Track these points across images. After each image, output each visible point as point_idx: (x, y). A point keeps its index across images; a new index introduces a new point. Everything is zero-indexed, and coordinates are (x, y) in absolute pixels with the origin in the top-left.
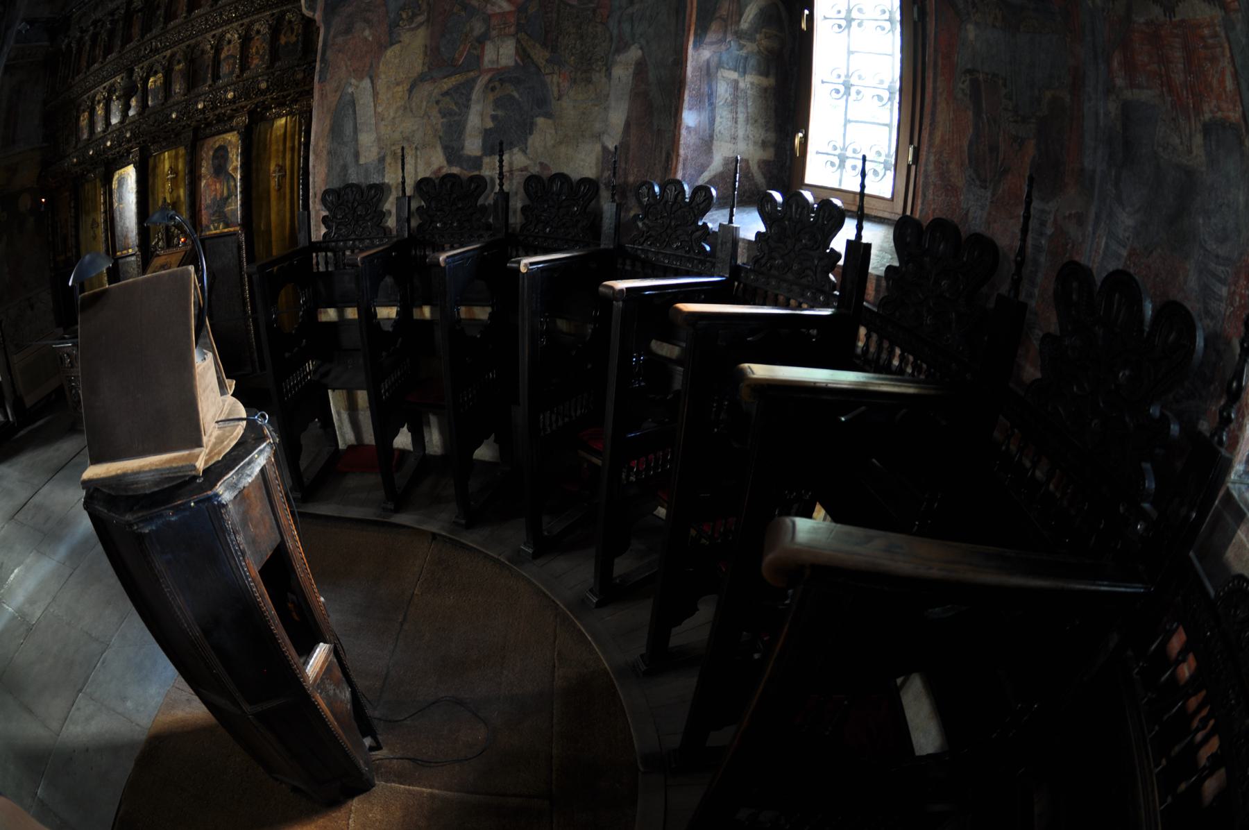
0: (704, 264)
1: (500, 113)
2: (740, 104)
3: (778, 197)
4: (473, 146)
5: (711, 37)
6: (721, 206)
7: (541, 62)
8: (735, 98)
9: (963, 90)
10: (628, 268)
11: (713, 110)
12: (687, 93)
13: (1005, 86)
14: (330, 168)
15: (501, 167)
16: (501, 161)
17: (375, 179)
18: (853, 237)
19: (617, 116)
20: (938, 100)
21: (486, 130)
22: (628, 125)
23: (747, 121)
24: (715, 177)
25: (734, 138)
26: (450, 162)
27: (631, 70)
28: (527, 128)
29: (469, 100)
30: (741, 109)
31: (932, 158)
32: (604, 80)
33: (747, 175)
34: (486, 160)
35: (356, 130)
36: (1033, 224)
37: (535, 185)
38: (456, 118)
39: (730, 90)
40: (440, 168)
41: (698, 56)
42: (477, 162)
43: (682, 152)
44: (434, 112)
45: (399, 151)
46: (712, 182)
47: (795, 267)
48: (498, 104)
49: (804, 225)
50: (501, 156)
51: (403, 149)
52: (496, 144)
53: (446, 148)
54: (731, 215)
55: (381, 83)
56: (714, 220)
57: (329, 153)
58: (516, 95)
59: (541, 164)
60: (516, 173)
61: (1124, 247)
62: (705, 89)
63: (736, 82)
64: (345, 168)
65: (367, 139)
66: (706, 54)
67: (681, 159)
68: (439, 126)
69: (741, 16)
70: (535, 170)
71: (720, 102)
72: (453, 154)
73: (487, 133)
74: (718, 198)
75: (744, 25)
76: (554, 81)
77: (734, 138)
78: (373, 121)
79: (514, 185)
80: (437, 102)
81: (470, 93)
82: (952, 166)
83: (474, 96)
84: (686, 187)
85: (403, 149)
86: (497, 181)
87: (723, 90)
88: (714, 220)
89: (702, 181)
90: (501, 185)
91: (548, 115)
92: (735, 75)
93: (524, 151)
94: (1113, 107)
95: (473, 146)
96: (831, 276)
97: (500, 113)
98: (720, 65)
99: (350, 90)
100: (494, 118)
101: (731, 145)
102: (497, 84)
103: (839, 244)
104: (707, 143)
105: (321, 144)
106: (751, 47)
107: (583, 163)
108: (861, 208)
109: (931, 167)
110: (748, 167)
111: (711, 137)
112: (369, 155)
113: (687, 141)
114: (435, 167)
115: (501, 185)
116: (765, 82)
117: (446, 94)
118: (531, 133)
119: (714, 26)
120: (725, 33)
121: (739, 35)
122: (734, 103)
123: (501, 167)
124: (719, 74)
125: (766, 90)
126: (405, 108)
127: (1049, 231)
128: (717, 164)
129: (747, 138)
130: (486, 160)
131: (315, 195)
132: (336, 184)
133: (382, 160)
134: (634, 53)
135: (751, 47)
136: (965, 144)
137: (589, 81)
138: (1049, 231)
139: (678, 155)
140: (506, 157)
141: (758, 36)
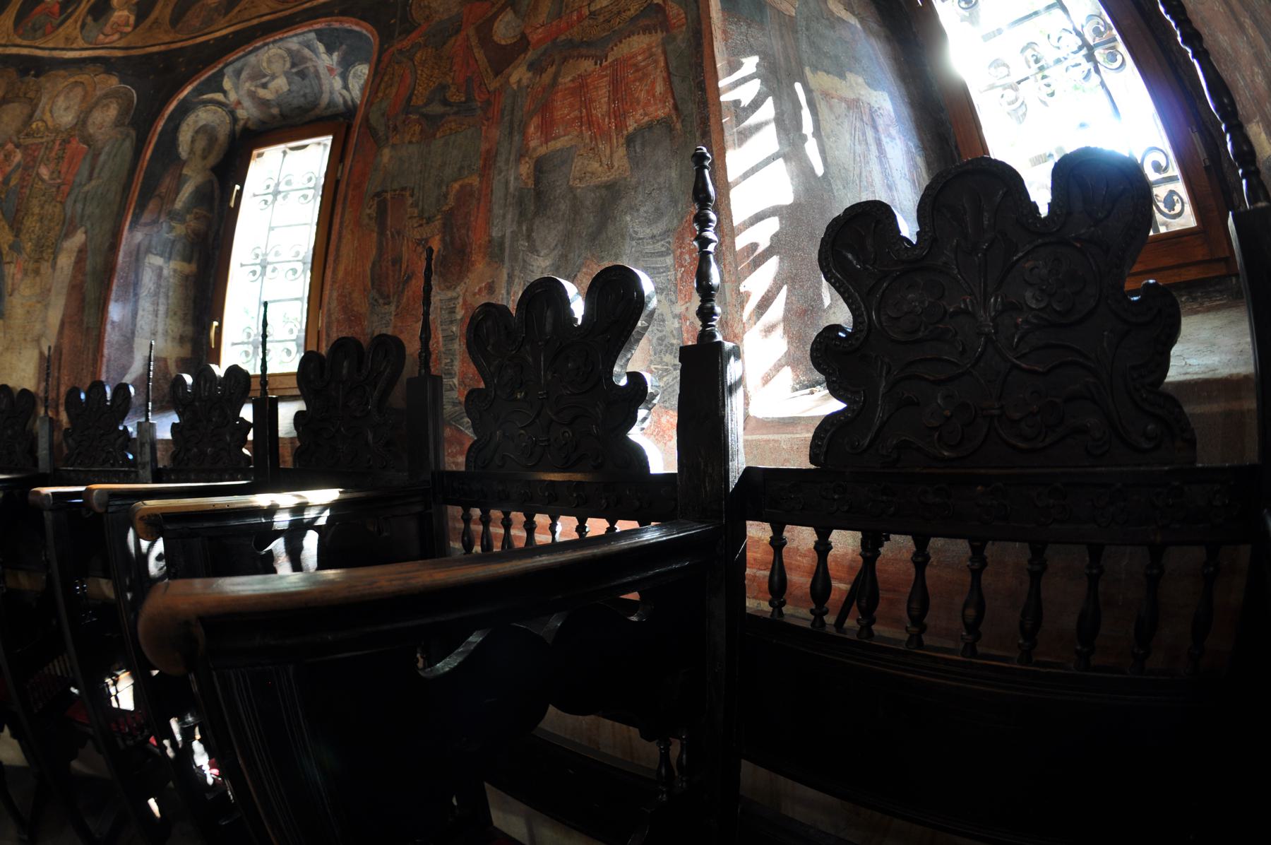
8: (159, 286)
11: (136, 302)
12: (115, 281)
25: (154, 334)
39: (155, 278)
63: (161, 269)
67: (105, 360)
71: (144, 292)
87: (148, 279)
111: (133, 333)
122: (156, 294)
135: (180, 229)
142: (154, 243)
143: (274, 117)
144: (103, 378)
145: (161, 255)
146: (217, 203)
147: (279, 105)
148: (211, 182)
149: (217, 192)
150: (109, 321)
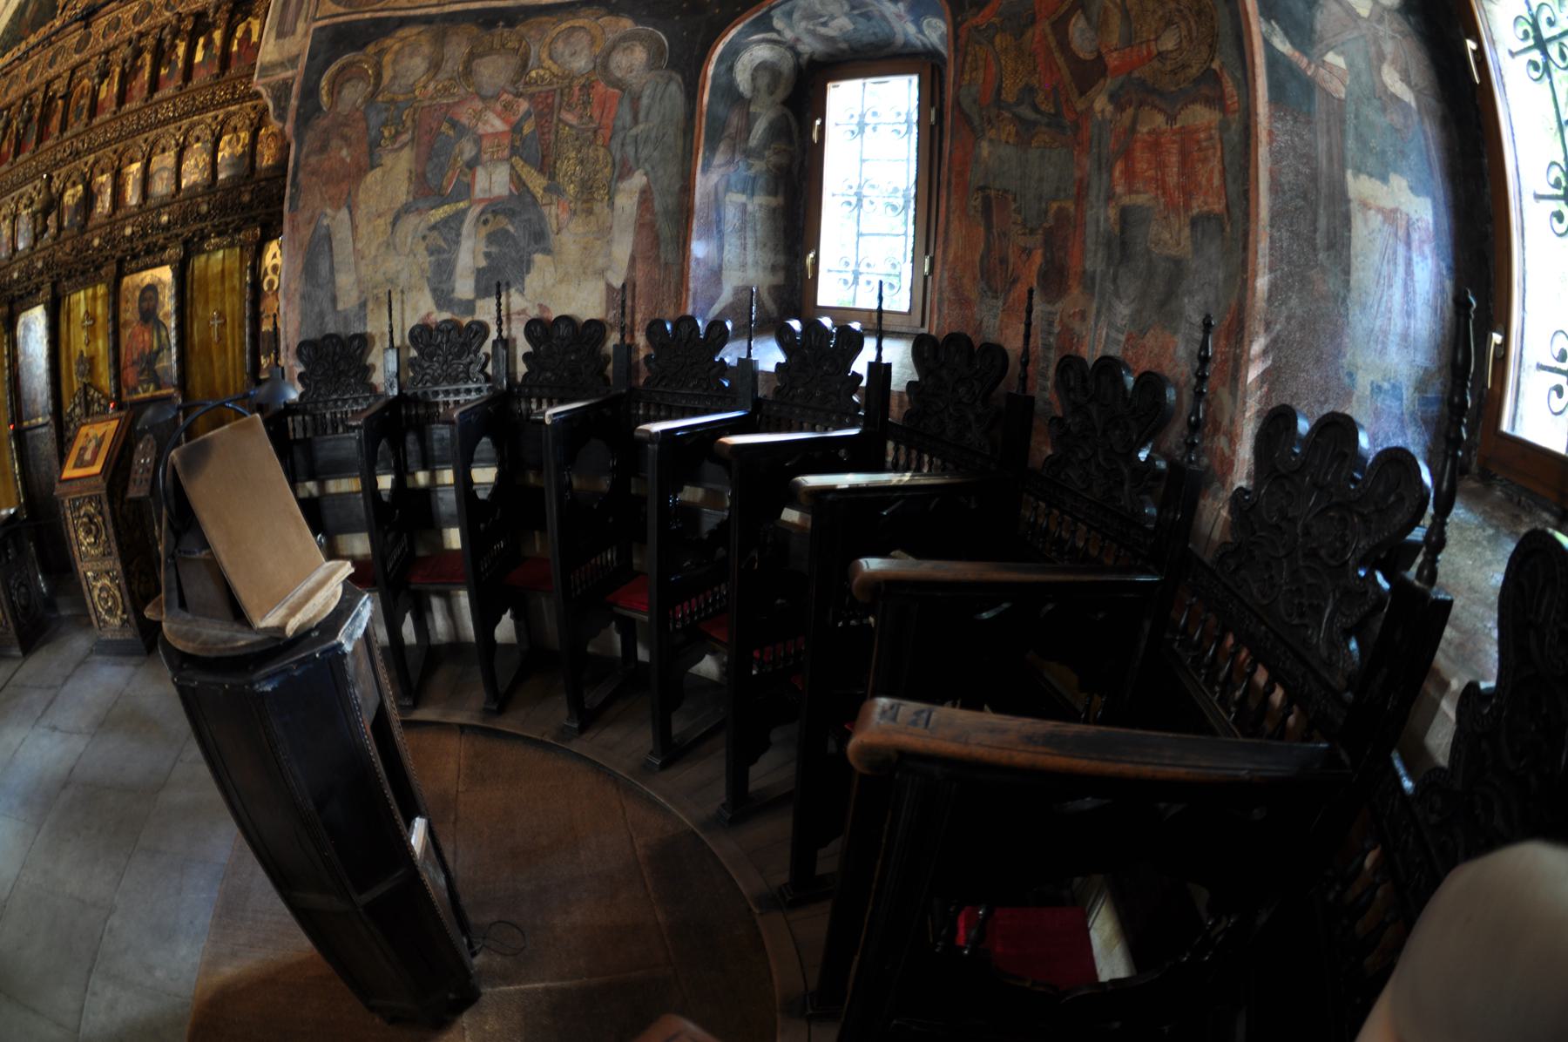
1: (494, 249)
4: (464, 288)
5: (719, 159)
7: (539, 192)
8: (744, 222)
14: (304, 315)
15: (499, 311)
16: (499, 304)
17: (356, 329)
22: (633, 259)
23: (756, 244)
25: (743, 266)
27: (636, 198)
28: (525, 266)
29: (459, 235)
32: (607, 210)
34: (480, 303)
35: (332, 270)
38: (445, 256)
39: (739, 214)
40: (428, 315)
41: (704, 184)
42: (469, 307)
43: (691, 285)
44: (421, 249)
48: (492, 238)
49: (823, 350)
50: (499, 299)
52: (494, 282)
53: (434, 291)
54: (750, 348)
56: (731, 355)
57: (303, 297)
58: (511, 228)
59: (540, 306)
63: (744, 205)
64: (321, 315)
66: (714, 177)
68: (426, 266)
69: (749, 132)
70: (534, 313)
72: (443, 298)
73: (480, 273)
75: (753, 142)
76: (553, 213)
80: (424, 238)
84: (700, 323)
87: (731, 216)
88: (731, 355)
90: (500, 330)
91: (547, 251)
92: (742, 198)
93: (521, 292)
95: (464, 288)
98: (728, 189)
100: (487, 255)
102: (490, 216)
103: (860, 366)
104: (716, 274)
105: (293, 286)
106: (759, 166)
107: (584, 302)
111: (720, 267)
112: (348, 300)
113: (696, 275)
114: (423, 313)
117: (433, 228)
118: (528, 272)
119: (722, 147)
121: (748, 154)
122: (743, 228)
123: (499, 311)
125: (774, 211)
126: (388, 245)
128: (726, 296)
129: (756, 263)
130: (480, 303)
131: (287, 348)
132: (313, 334)
133: (363, 305)
134: (638, 180)
135: (759, 166)
137: (590, 212)
140: (503, 300)
143: (843, 51)
144: (689, 312)
145: (743, 191)
146: (796, 136)
147: (846, 41)
148: (785, 115)
149: (794, 125)
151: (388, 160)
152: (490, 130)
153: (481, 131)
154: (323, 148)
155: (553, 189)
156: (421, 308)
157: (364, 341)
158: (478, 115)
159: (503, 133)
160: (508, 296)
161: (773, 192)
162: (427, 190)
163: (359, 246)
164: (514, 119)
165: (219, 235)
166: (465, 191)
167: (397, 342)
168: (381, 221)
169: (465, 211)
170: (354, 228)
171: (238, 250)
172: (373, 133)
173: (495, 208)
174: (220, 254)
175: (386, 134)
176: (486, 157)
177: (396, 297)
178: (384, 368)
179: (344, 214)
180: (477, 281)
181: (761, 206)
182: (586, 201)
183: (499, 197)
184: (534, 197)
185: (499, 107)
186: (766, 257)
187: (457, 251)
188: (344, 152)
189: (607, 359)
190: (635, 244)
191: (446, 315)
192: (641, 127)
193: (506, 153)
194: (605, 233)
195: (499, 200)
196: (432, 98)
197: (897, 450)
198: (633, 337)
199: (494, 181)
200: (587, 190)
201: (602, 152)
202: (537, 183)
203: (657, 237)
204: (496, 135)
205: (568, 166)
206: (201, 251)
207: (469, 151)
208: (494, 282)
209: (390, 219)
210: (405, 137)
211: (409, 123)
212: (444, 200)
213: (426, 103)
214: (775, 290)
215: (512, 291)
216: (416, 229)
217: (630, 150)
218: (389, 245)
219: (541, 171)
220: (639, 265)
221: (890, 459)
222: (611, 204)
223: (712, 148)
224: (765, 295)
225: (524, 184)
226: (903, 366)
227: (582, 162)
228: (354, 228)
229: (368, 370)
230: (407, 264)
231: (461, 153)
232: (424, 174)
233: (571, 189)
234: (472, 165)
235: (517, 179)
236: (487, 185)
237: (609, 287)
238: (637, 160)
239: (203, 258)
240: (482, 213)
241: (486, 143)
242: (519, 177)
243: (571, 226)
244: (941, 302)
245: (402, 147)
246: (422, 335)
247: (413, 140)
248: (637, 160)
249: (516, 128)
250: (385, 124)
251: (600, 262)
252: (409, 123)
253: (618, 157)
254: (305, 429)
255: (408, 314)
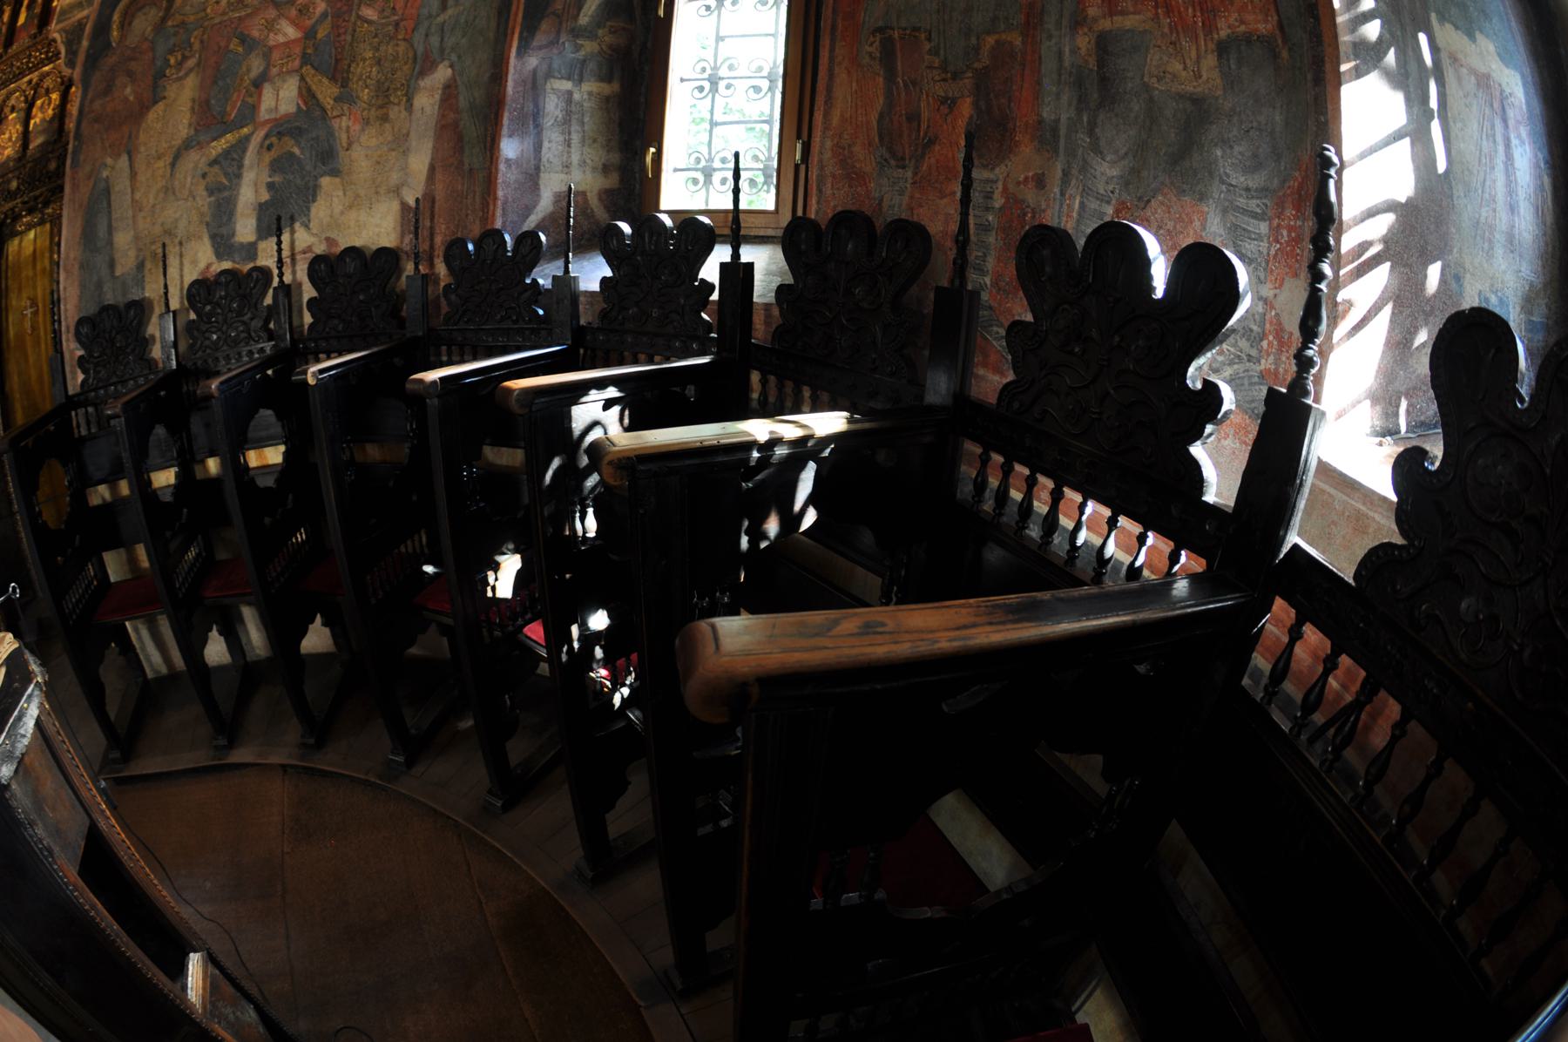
0: (537, 333)
1: (277, 179)
2: (574, 122)
3: (626, 228)
4: (245, 229)
5: (540, 39)
6: (554, 257)
7: (328, 102)
8: (568, 113)
9: (870, 54)
10: (445, 358)
12: (506, 115)
13: (929, 39)
14: (83, 286)
15: (280, 251)
16: (279, 243)
17: (135, 295)
18: (728, 259)
19: (419, 161)
20: (837, 70)
21: (261, 205)
22: (432, 169)
23: (583, 141)
24: (544, 219)
26: (220, 256)
27: (437, 97)
28: (310, 193)
29: (241, 167)
30: (575, 127)
31: (829, 144)
32: (404, 114)
33: (584, 210)
34: (262, 245)
35: (110, 230)
36: (976, 196)
37: (324, 268)
38: (226, 194)
40: (208, 267)
41: (520, 66)
42: (251, 250)
43: (500, 193)
44: (201, 191)
45: (160, 251)
46: (542, 226)
47: (655, 313)
48: (275, 167)
49: (661, 257)
50: (279, 237)
51: (164, 245)
53: (213, 237)
54: (567, 263)
55: (140, 159)
58: (296, 151)
59: (328, 239)
60: (298, 257)
61: (1108, 202)
62: (530, 107)
63: (570, 93)
64: (99, 285)
65: (122, 239)
66: (533, 61)
68: (205, 209)
69: (580, 9)
70: (320, 249)
71: (548, 122)
72: (223, 244)
73: (262, 208)
74: (550, 247)
76: (343, 125)
77: (567, 167)
78: (130, 213)
79: (300, 273)
80: (204, 176)
81: (242, 158)
82: (857, 149)
83: (247, 162)
84: (507, 238)
85: (164, 245)
86: (276, 272)
87: (552, 106)
88: (544, 276)
89: (530, 223)
90: (281, 275)
91: (335, 173)
92: (567, 85)
93: (307, 227)
94: (1084, 42)
95: (245, 229)
96: (704, 316)
97: (277, 179)
98: (549, 75)
99: (105, 174)
100: (271, 186)
101: (563, 176)
102: (274, 140)
103: (710, 271)
106: (590, 47)
107: (377, 228)
108: (735, 227)
109: (828, 155)
110: (586, 201)
112: (126, 263)
113: (507, 177)
114: (202, 265)
115: (281, 275)
116: (606, 89)
119: (544, 26)
120: (558, 33)
121: (576, 33)
122: (566, 122)
123: (280, 251)
124: (548, 86)
125: (607, 99)
126: (167, 189)
127: (998, 202)
128: (546, 203)
130: (262, 245)
133: (140, 266)
134: (443, 73)
135: (590, 47)
136: (874, 118)
137: (385, 119)
138: (998, 202)
139: (496, 199)
140: (285, 237)
141: (600, 32)
142: (555, 66)
145: (569, 79)
150: (502, 159)
151: (171, 91)
152: (281, 39)
153: (272, 43)
154: (108, 90)
155: (346, 98)
156: (201, 260)
157: (140, 308)
158: (270, 26)
159: (294, 41)
160: (293, 232)
161: (607, 78)
162: (210, 119)
163: (138, 196)
164: (309, 23)
165: (30, 212)
166: (249, 113)
167: (175, 304)
168: (161, 164)
169: (247, 138)
170: (133, 175)
171: (48, 226)
172: (159, 63)
173: (283, 128)
174: (32, 234)
175: (172, 61)
176: (274, 71)
177: (172, 252)
178: (162, 335)
179: (124, 159)
180: (259, 220)
181: (590, 94)
182: (381, 107)
183: (286, 115)
184: (324, 110)
185: (294, 12)
186: (596, 155)
187: (238, 185)
188: (128, 90)
189: (401, 298)
190: (435, 149)
191: (227, 265)
192: (450, 12)
193: (297, 63)
194: (401, 143)
195: (287, 118)
196: (224, 13)
197: (764, 382)
198: (432, 265)
199: (281, 98)
200: (383, 95)
201: (402, 47)
202: (326, 92)
203: (460, 138)
204: (287, 44)
205: (364, 70)
206: (14, 234)
207: (256, 65)
208: (274, 222)
209: (169, 160)
210: (191, 63)
211: (197, 46)
212: (226, 127)
213: (217, 21)
214: (607, 196)
215: (297, 225)
216: (196, 167)
217: (435, 40)
218: (168, 190)
219: (333, 79)
220: (439, 176)
221: (755, 396)
222: (409, 107)
223: (530, 28)
224: (594, 202)
225: (314, 96)
226: (768, 273)
227: (379, 63)
228: (133, 175)
229: (146, 343)
230: (186, 212)
231: (249, 70)
232: (207, 102)
233: (365, 94)
234: (258, 84)
235: (307, 94)
236: (273, 104)
237: (404, 206)
238: (442, 50)
239: (16, 241)
240: (267, 136)
241: (276, 55)
242: (309, 90)
243: (363, 139)
244: (821, 180)
245: (187, 75)
246: (200, 291)
247: (198, 64)
248: (442, 50)
249: (310, 34)
250: (171, 52)
251: (395, 177)
252: (197, 46)
253: (420, 50)
254: (88, 423)
255: (186, 270)
